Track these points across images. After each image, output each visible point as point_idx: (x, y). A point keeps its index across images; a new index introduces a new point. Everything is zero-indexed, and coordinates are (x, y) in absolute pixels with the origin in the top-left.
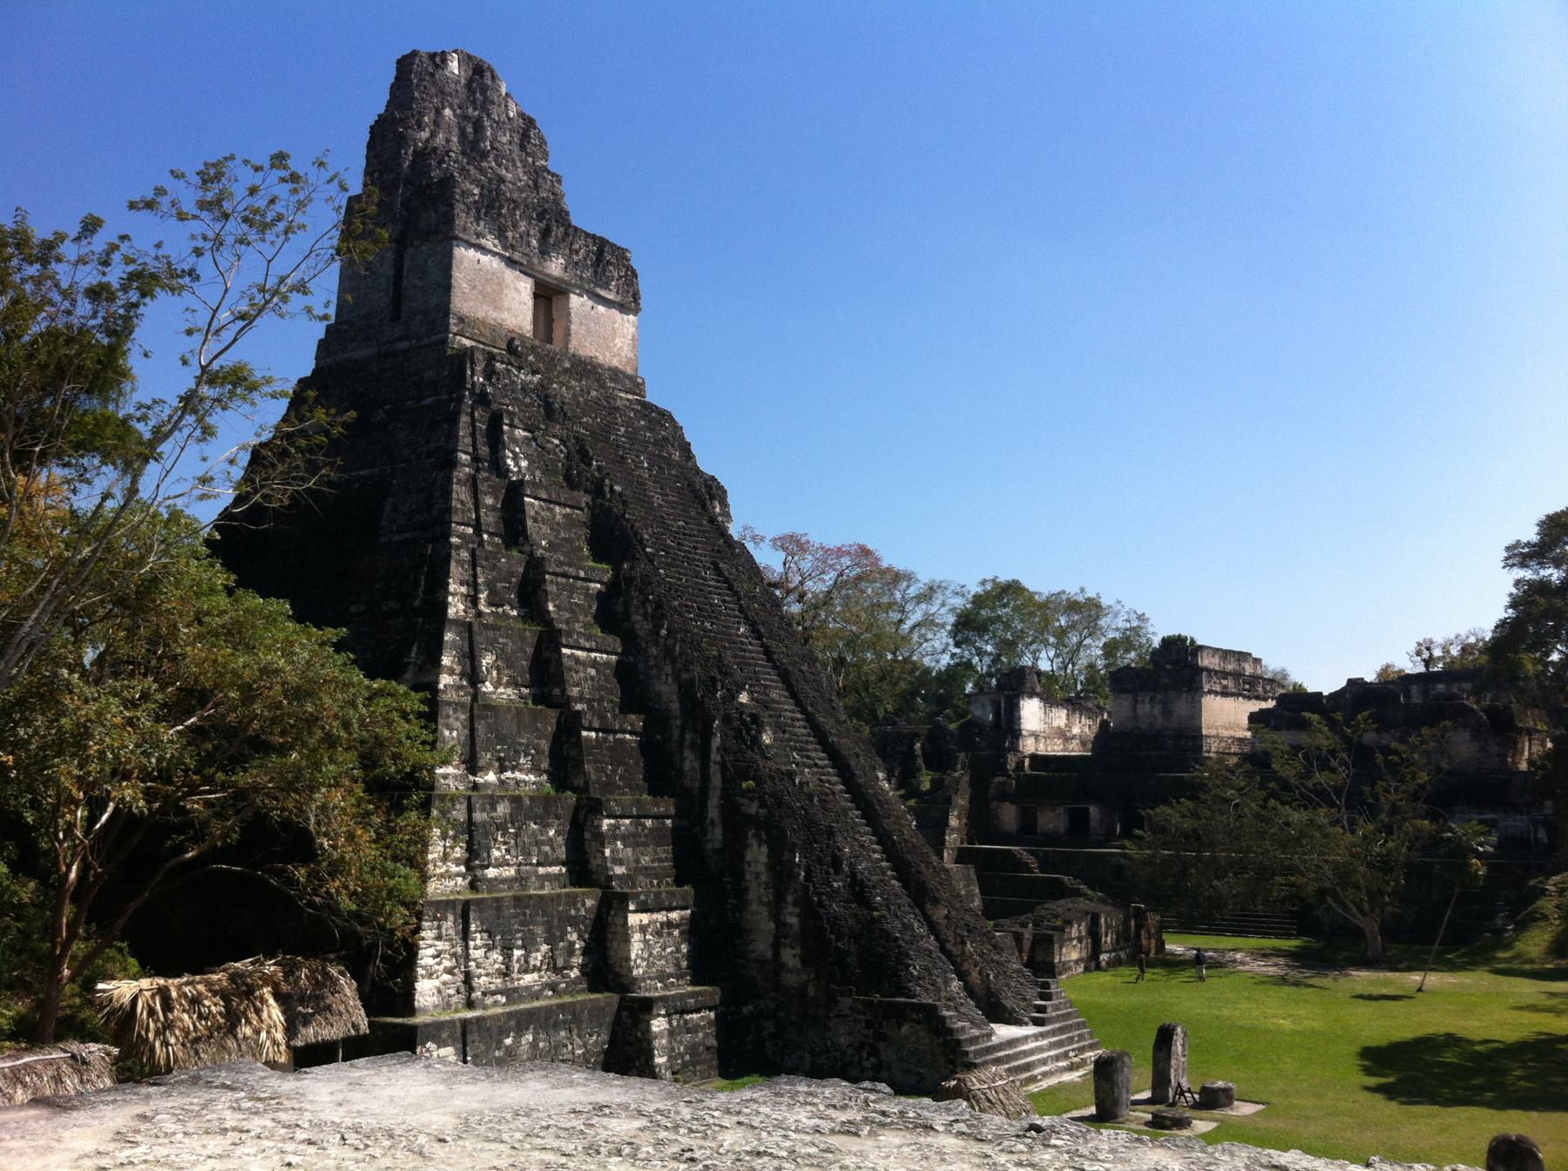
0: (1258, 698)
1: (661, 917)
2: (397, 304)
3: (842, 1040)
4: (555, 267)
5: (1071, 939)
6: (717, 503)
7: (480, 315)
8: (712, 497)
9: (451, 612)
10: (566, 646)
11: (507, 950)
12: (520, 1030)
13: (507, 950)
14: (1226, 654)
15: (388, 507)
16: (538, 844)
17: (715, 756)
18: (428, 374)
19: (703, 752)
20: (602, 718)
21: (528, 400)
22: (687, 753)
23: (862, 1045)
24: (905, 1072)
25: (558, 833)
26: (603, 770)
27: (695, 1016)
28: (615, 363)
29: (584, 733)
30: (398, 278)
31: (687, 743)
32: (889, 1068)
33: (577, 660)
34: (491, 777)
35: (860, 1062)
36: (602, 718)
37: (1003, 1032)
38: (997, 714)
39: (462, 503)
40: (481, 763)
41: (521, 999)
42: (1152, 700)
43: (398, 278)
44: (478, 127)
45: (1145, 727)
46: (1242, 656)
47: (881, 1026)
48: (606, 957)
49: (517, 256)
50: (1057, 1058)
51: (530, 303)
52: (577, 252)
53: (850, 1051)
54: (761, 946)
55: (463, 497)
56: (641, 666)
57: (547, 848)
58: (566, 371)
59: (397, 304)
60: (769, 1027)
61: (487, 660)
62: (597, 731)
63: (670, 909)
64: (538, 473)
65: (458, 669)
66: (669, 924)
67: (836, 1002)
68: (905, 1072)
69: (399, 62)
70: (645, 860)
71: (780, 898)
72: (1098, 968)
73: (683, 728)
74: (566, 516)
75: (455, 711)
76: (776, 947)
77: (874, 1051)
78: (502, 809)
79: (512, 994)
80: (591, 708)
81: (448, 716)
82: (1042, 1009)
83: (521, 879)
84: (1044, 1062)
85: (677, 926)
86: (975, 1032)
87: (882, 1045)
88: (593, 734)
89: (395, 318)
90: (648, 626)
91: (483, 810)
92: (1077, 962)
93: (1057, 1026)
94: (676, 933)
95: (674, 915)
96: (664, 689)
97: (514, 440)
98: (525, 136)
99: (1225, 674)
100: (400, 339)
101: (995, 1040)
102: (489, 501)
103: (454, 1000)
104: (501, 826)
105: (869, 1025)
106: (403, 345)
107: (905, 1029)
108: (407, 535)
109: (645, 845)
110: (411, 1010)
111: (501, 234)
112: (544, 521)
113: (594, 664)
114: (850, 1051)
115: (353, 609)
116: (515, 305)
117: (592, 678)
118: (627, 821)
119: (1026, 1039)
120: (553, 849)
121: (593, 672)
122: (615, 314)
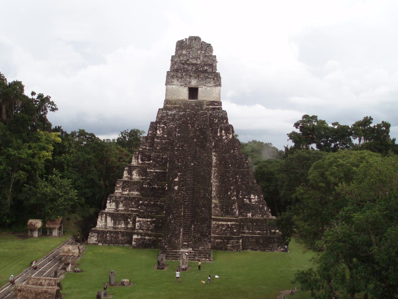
4: (194, 83)
10: (148, 169)
25: (134, 203)
28: (213, 100)
29: (144, 186)
33: (151, 172)
34: (126, 193)
41: (116, 229)
44: (189, 53)
49: (183, 84)
55: (144, 141)
61: (134, 173)
62: (148, 185)
63: (148, 218)
66: (147, 221)
75: (120, 182)
85: (149, 222)
88: (147, 186)
95: (149, 220)
97: (160, 127)
111: (178, 80)
113: (156, 172)
117: (154, 175)
118: (146, 202)
121: (155, 174)
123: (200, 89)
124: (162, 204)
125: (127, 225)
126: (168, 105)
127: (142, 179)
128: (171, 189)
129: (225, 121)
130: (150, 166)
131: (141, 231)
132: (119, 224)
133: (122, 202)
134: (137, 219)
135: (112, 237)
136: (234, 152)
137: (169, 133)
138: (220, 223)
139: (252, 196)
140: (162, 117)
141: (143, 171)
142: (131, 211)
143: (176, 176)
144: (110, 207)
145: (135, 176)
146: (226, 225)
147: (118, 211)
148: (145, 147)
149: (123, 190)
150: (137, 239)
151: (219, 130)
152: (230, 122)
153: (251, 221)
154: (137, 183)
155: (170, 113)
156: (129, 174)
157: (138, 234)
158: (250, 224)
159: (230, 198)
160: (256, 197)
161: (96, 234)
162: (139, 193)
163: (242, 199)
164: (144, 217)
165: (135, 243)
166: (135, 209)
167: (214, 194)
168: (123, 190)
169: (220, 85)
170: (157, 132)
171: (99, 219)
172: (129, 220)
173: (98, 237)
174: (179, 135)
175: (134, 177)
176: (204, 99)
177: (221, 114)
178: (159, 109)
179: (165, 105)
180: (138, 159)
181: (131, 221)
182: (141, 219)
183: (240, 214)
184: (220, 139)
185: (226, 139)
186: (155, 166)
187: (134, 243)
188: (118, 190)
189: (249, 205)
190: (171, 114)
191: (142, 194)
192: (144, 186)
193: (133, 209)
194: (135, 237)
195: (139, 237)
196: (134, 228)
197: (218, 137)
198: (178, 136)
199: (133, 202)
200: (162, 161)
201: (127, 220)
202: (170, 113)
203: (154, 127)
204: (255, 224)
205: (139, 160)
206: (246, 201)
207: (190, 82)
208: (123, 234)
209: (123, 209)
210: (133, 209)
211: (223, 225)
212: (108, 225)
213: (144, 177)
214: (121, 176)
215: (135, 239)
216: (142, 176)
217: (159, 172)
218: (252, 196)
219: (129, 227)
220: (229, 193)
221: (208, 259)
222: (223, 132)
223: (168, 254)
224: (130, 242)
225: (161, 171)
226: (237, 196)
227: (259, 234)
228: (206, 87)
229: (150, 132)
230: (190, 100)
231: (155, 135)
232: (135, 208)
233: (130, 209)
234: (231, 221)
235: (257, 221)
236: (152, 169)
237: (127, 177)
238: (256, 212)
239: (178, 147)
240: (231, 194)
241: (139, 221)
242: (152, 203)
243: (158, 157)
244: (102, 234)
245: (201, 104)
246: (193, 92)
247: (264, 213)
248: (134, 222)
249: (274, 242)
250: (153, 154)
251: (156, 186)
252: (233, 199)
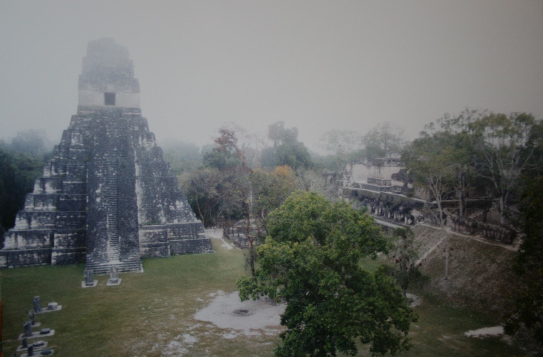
4: (110, 89)
33: (68, 184)
61: (47, 185)
66: (68, 236)
88: (64, 199)
94: (70, 238)
95: (69, 235)
97: (74, 135)
102: (63, 150)
113: (74, 184)
118: (65, 217)
121: (72, 186)
123: (117, 96)
125: (43, 243)
126: (81, 111)
127: (58, 192)
128: (93, 200)
129: (146, 129)
130: (64, 177)
131: (61, 248)
132: (33, 243)
133: (35, 218)
134: (56, 235)
135: (26, 257)
136: (157, 160)
137: (86, 141)
138: (148, 231)
139: (177, 203)
140: (76, 125)
141: (58, 183)
142: (47, 227)
143: (97, 187)
144: (20, 224)
145: (50, 190)
146: (153, 232)
147: (30, 228)
149: (35, 205)
150: (57, 256)
151: (140, 138)
152: (151, 130)
153: (178, 226)
154: (52, 196)
155: (86, 120)
157: (58, 251)
158: (177, 229)
159: (155, 206)
160: (182, 203)
163: (168, 206)
164: (64, 232)
167: (139, 203)
168: (35, 205)
169: (138, 91)
170: (70, 141)
171: (7, 239)
172: (45, 237)
173: (7, 259)
174: (97, 144)
177: (142, 122)
178: (73, 116)
179: (78, 111)
180: (51, 169)
181: (48, 237)
183: (168, 220)
184: (143, 148)
185: (148, 147)
186: (72, 179)
187: (53, 261)
188: (28, 205)
189: (175, 211)
190: (87, 122)
191: (58, 208)
192: (61, 199)
193: (49, 225)
194: (54, 254)
195: (60, 254)
196: (52, 244)
197: (139, 145)
198: (97, 145)
201: (43, 238)
202: (86, 120)
203: (67, 135)
204: (181, 229)
206: (172, 208)
208: (39, 253)
211: (150, 233)
214: (32, 190)
217: (79, 184)
218: (177, 203)
220: (154, 201)
221: (138, 269)
222: (145, 140)
224: (48, 260)
226: (163, 205)
227: (186, 238)
229: (63, 141)
230: (107, 106)
231: (70, 143)
234: (157, 228)
235: (183, 226)
236: (68, 181)
237: (39, 191)
238: (182, 217)
239: (98, 157)
240: (156, 201)
241: (59, 237)
242: (72, 217)
243: (75, 167)
245: (119, 112)
246: (110, 98)
247: (189, 218)
248: (52, 238)
249: (201, 245)
250: (69, 165)
251: (75, 199)
252: (158, 206)
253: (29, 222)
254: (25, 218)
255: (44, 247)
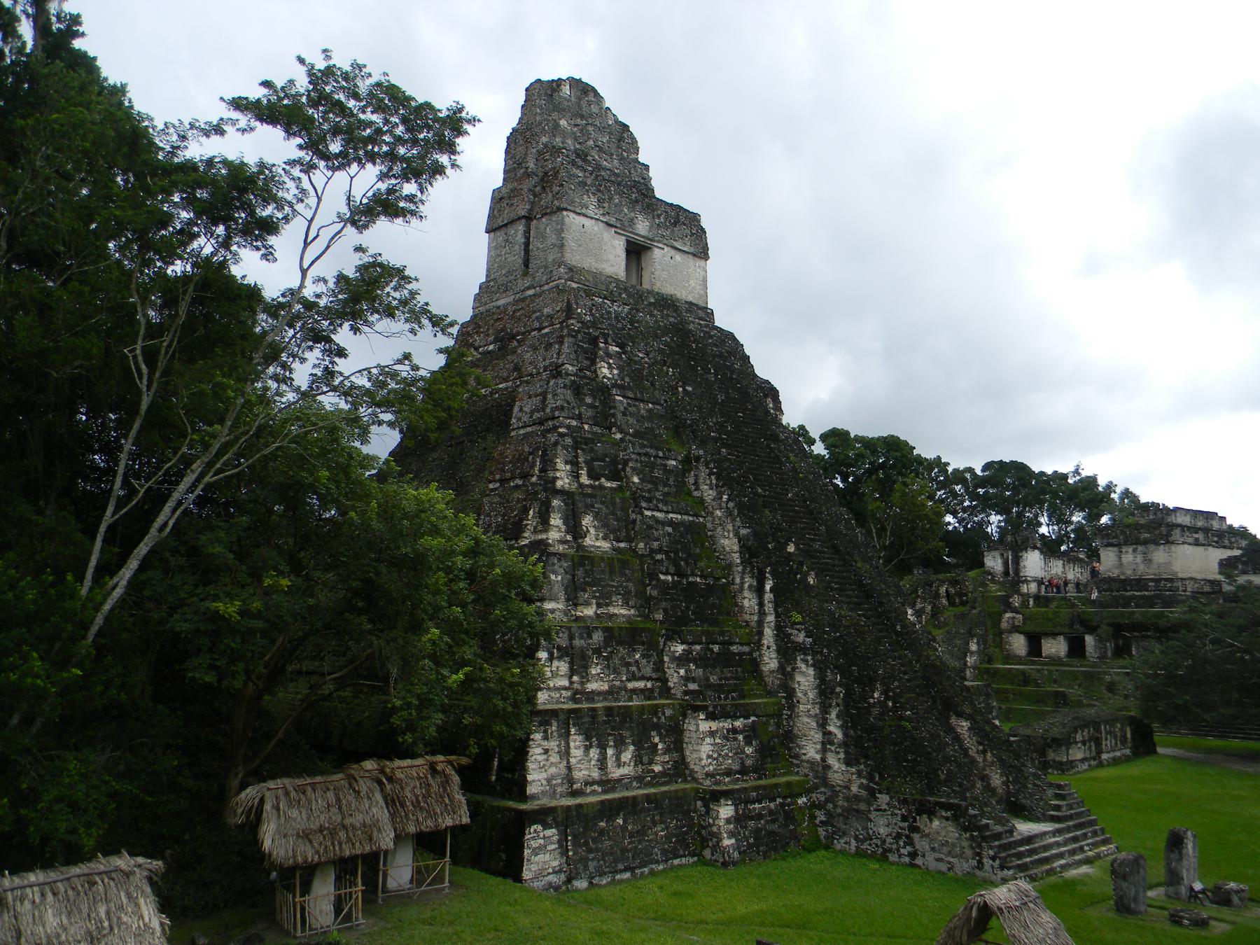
0: (1224, 547)
1: (727, 724)
2: (526, 264)
3: (882, 831)
4: (642, 227)
5: (1076, 743)
6: (769, 400)
7: (586, 266)
8: (766, 396)
9: (559, 484)
11: (603, 747)
12: (611, 818)
13: (603, 747)
14: (1196, 514)
15: (516, 409)
16: (628, 665)
17: (768, 596)
18: (546, 311)
19: (760, 591)
20: (677, 566)
21: (620, 325)
22: (746, 593)
23: (898, 836)
24: (937, 860)
25: (643, 656)
26: (679, 606)
27: (757, 806)
28: (690, 299)
29: (662, 577)
30: (527, 244)
31: (746, 585)
32: (924, 856)
33: (657, 521)
34: (589, 611)
35: (898, 850)
36: (677, 566)
37: (1025, 828)
38: (1006, 563)
39: (568, 403)
40: (581, 600)
41: (613, 789)
42: (1135, 550)
43: (527, 244)
45: (1129, 572)
46: (1210, 515)
47: (915, 820)
48: (683, 758)
49: (613, 221)
50: (1073, 852)
51: (623, 255)
52: (659, 216)
53: (889, 840)
54: (811, 751)
56: (709, 525)
57: (634, 668)
58: (651, 304)
59: (526, 264)
60: (821, 816)
61: (587, 521)
62: (672, 575)
63: (735, 718)
64: (627, 379)
65: (563, 528)
66: (734, 731)
67: (876, 799)
68: (937, 860)
69: (527, 90)
70: (713, 679)
71: (825, 709)
72: (1101, 765)
73: (743, 572)
74: (650, 411)
75: (559, 560)
76: (824, 750)
77: (910, 842)
78: (597, 637)
79: (608, 784)
80: (668, 558)
81: (554, 564)
82: (1058, 808)
83: (612, 693)
84: (1061, 856)
85: (741, 732)
86: (999, 828)
87: (916, 836)
88: (670, 578)
89: (525, 274)
90: (713, 493)
91: (581, 637)
92: (1082, 761)
93: (1071, 823)
94: (741, 737)
95: (738, 723)
96: (726, 542)
98: (621, 139)
99: (1195, 530)
100: (528, 288)
101: (1016, 837)
103: (559, 790)
104: (597, 651)
105: (904, 819)
106: (531, 292)
107: (936, 823)
108: (529, 429)
109: (714, 667)
110: (523, 797)
112: (632, 415)
113: (671, 523)
114: (889, 840)
115: (491, 486)
116: (611, 257)
117: (669, 534)
119: (1045, 833)
120: (639, 669)
121: (670, 530)
122: (690, 261)
123: (657, 253)
124: (744, 653)
133: (597, 651)
148: (574, 423)
156: (567, 532)
161: (554, 830)
162: (632, 611)
165: (733, 841)
166: (649, 685)
175: (588, 541)
176: (668, 290)
182: (714, 725)
193: (640, 684)
199: (634, 650)
200: (668, 479)
205: (583, 472)
207: (632, 220)
209: (605, 687)
210: (640, 684)
212: (578, 775)
213: (622, 545)
215: (728, 821)
216: (618, 541)
219: (657, 768)
223: (1020, 855)
224: (695, 840)
225: (685, 517)
228: (673, 252)
232: (648, 679)
233: (630, 685)
241: (712, 734)
242: (716, 648)
244: (574, 823)
253: (579, 665)
254: (565, 652)
255: (656, 779)
